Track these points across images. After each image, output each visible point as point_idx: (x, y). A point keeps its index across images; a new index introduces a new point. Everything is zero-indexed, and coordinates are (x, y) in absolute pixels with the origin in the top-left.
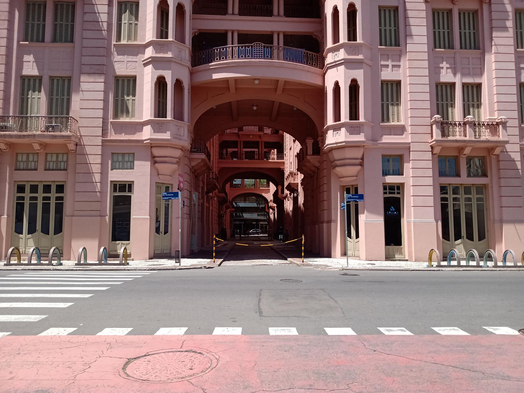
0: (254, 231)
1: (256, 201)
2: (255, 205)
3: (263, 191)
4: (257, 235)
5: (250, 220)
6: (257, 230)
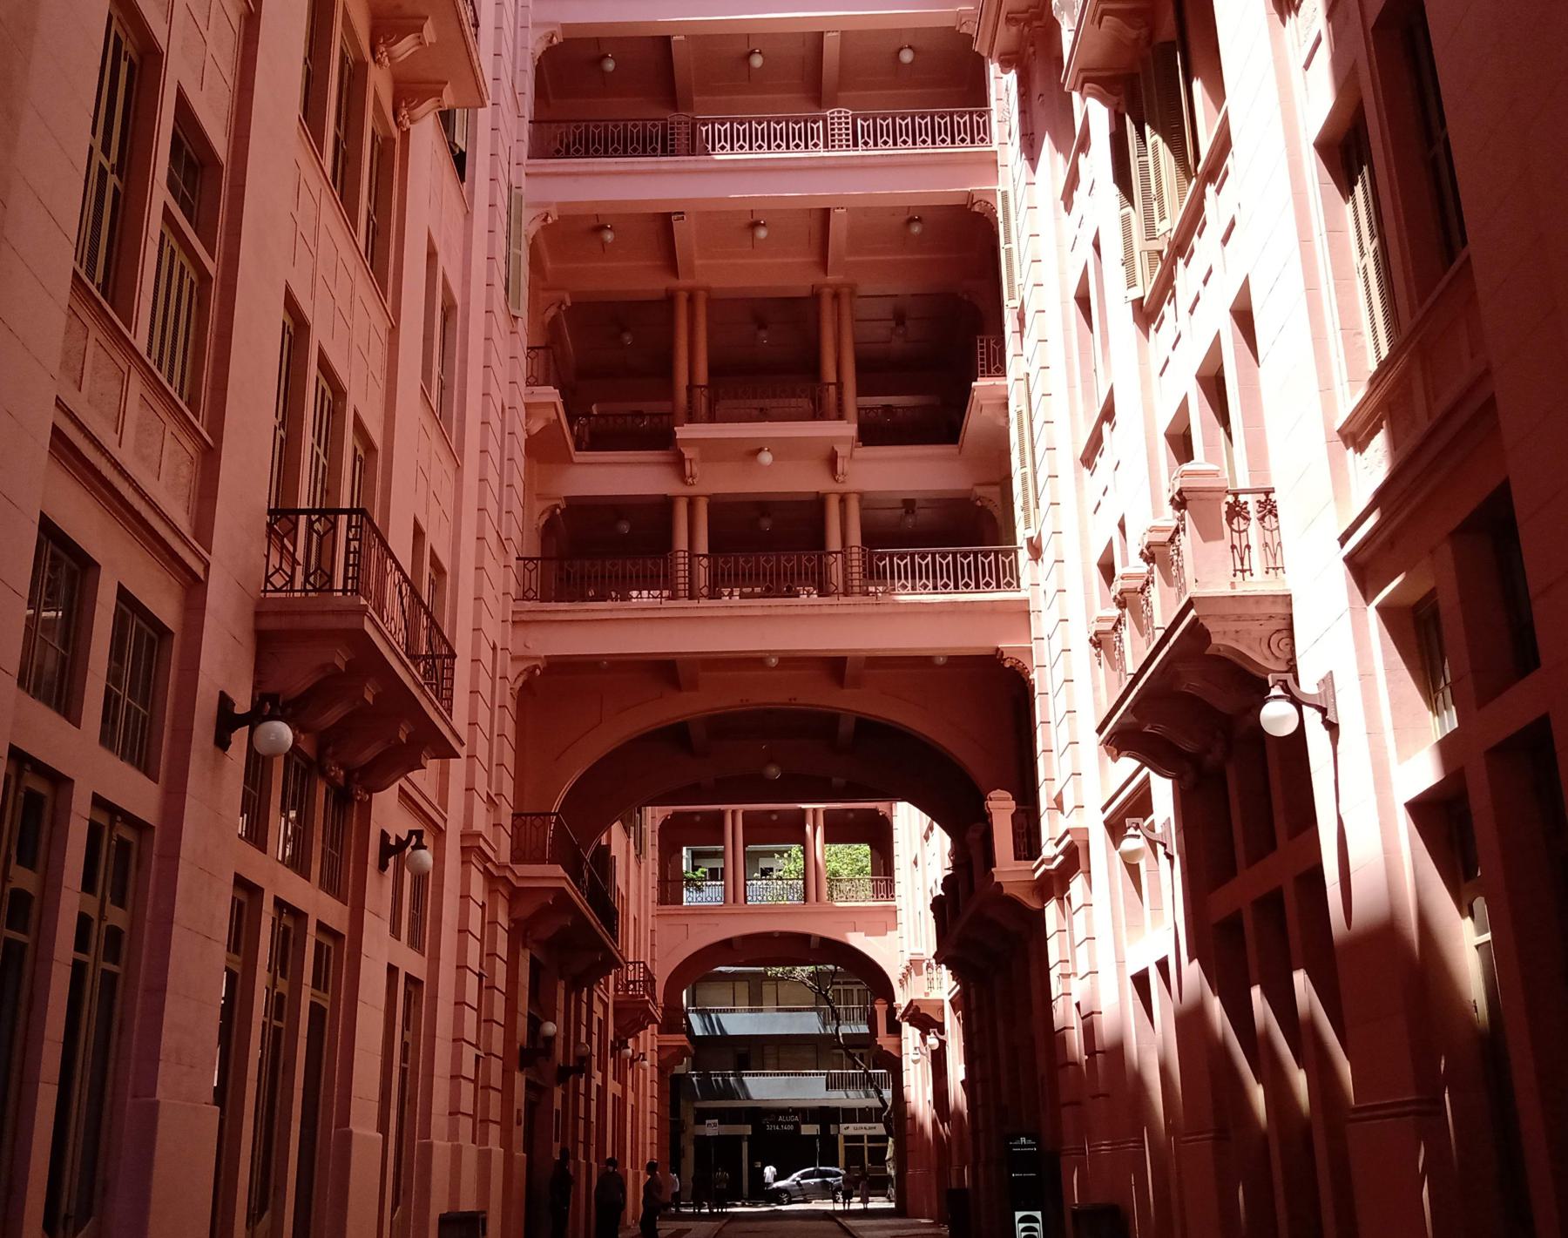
0: (812, 1181)
1: (822, 997)
2: (808, 1023)
3: (856, 918)
4: (827, 1205)
5: (785, 1112)
6: (830, 1174)
